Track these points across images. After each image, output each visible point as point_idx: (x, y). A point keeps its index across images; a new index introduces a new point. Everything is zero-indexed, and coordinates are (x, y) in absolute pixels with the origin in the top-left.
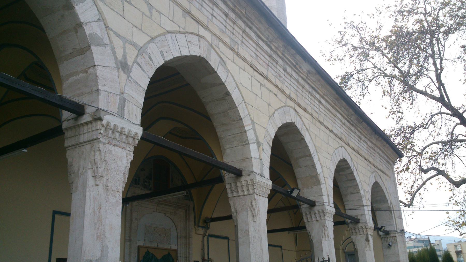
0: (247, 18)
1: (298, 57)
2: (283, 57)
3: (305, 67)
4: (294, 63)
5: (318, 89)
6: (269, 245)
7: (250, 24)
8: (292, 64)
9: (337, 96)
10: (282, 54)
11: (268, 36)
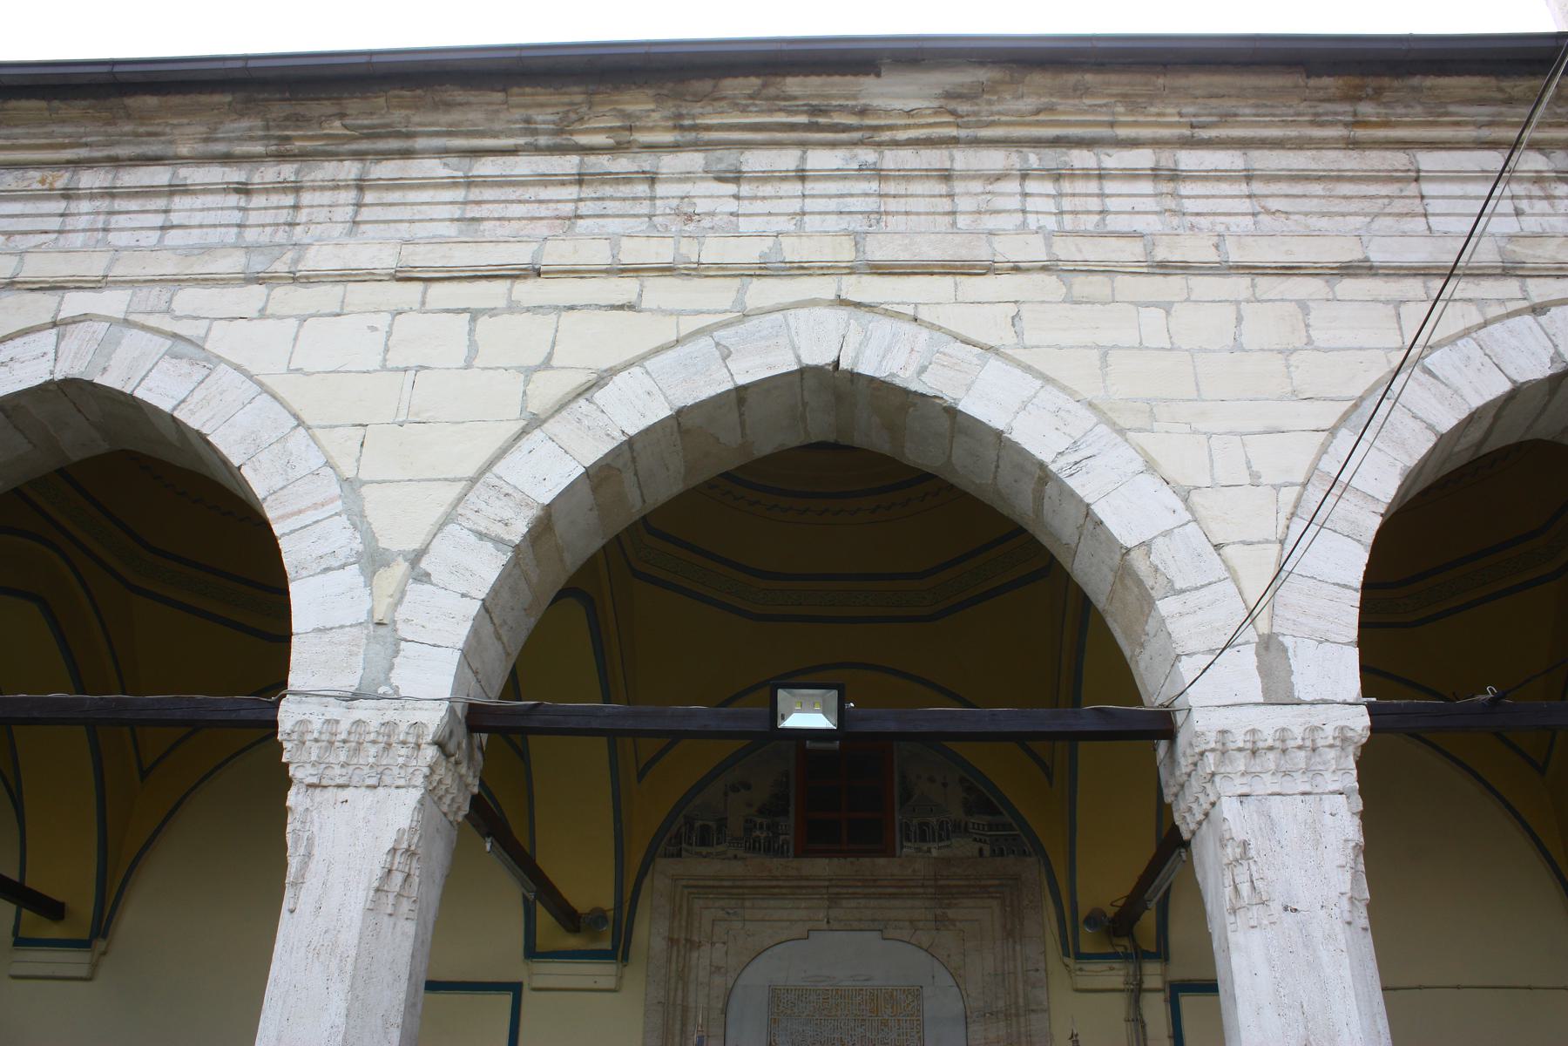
0: (368, 137)
1: (793, 85)
2: (690, 136)
3: (891, 94)
4: (803, 119)
5: (1112, 124)
6: (1384, 989)
7: (394, 144)
8: (793, 127)
9: (1326, 81)
10: (682, 128)
11: (528, 121)
